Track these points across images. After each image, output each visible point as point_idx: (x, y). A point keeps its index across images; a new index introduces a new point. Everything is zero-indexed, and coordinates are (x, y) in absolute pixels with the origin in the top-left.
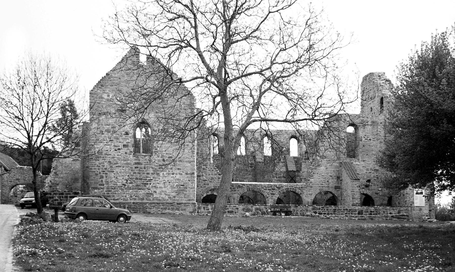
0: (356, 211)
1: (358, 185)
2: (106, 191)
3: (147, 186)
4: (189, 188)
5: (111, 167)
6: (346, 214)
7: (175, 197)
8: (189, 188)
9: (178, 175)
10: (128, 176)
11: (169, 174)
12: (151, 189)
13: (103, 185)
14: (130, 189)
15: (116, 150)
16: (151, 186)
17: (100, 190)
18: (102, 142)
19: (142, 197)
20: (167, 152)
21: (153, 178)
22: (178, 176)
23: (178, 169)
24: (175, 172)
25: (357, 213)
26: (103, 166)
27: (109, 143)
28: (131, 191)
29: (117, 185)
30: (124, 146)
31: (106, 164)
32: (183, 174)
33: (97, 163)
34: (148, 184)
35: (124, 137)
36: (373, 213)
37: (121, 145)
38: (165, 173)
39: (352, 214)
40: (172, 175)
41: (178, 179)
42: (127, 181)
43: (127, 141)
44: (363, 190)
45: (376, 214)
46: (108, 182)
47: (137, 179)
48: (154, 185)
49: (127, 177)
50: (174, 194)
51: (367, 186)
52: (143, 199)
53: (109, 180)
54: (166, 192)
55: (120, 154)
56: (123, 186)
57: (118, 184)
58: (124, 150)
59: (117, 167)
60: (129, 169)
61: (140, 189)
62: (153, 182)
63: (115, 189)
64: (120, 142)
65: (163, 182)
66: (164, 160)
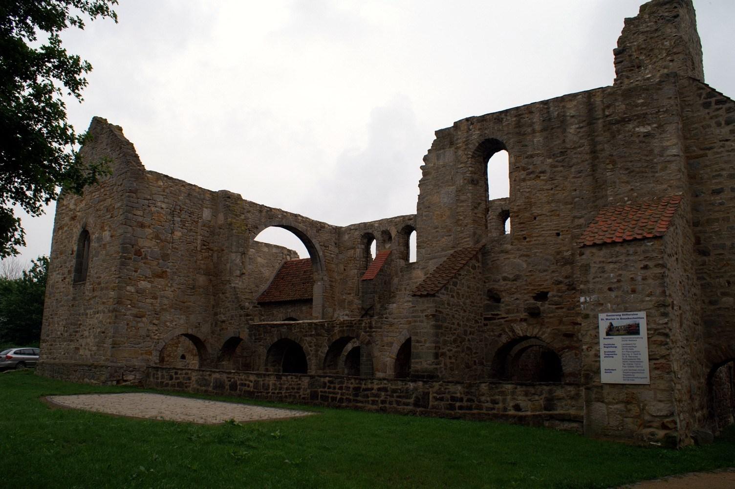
0: (407, 394)
1: (429, 312)
6: (383, 402)
25: (412, 401)
36: (458, 404)
39: (398, 403)
44: (525, 324)
45: (470, 408)
51: (534, 313)
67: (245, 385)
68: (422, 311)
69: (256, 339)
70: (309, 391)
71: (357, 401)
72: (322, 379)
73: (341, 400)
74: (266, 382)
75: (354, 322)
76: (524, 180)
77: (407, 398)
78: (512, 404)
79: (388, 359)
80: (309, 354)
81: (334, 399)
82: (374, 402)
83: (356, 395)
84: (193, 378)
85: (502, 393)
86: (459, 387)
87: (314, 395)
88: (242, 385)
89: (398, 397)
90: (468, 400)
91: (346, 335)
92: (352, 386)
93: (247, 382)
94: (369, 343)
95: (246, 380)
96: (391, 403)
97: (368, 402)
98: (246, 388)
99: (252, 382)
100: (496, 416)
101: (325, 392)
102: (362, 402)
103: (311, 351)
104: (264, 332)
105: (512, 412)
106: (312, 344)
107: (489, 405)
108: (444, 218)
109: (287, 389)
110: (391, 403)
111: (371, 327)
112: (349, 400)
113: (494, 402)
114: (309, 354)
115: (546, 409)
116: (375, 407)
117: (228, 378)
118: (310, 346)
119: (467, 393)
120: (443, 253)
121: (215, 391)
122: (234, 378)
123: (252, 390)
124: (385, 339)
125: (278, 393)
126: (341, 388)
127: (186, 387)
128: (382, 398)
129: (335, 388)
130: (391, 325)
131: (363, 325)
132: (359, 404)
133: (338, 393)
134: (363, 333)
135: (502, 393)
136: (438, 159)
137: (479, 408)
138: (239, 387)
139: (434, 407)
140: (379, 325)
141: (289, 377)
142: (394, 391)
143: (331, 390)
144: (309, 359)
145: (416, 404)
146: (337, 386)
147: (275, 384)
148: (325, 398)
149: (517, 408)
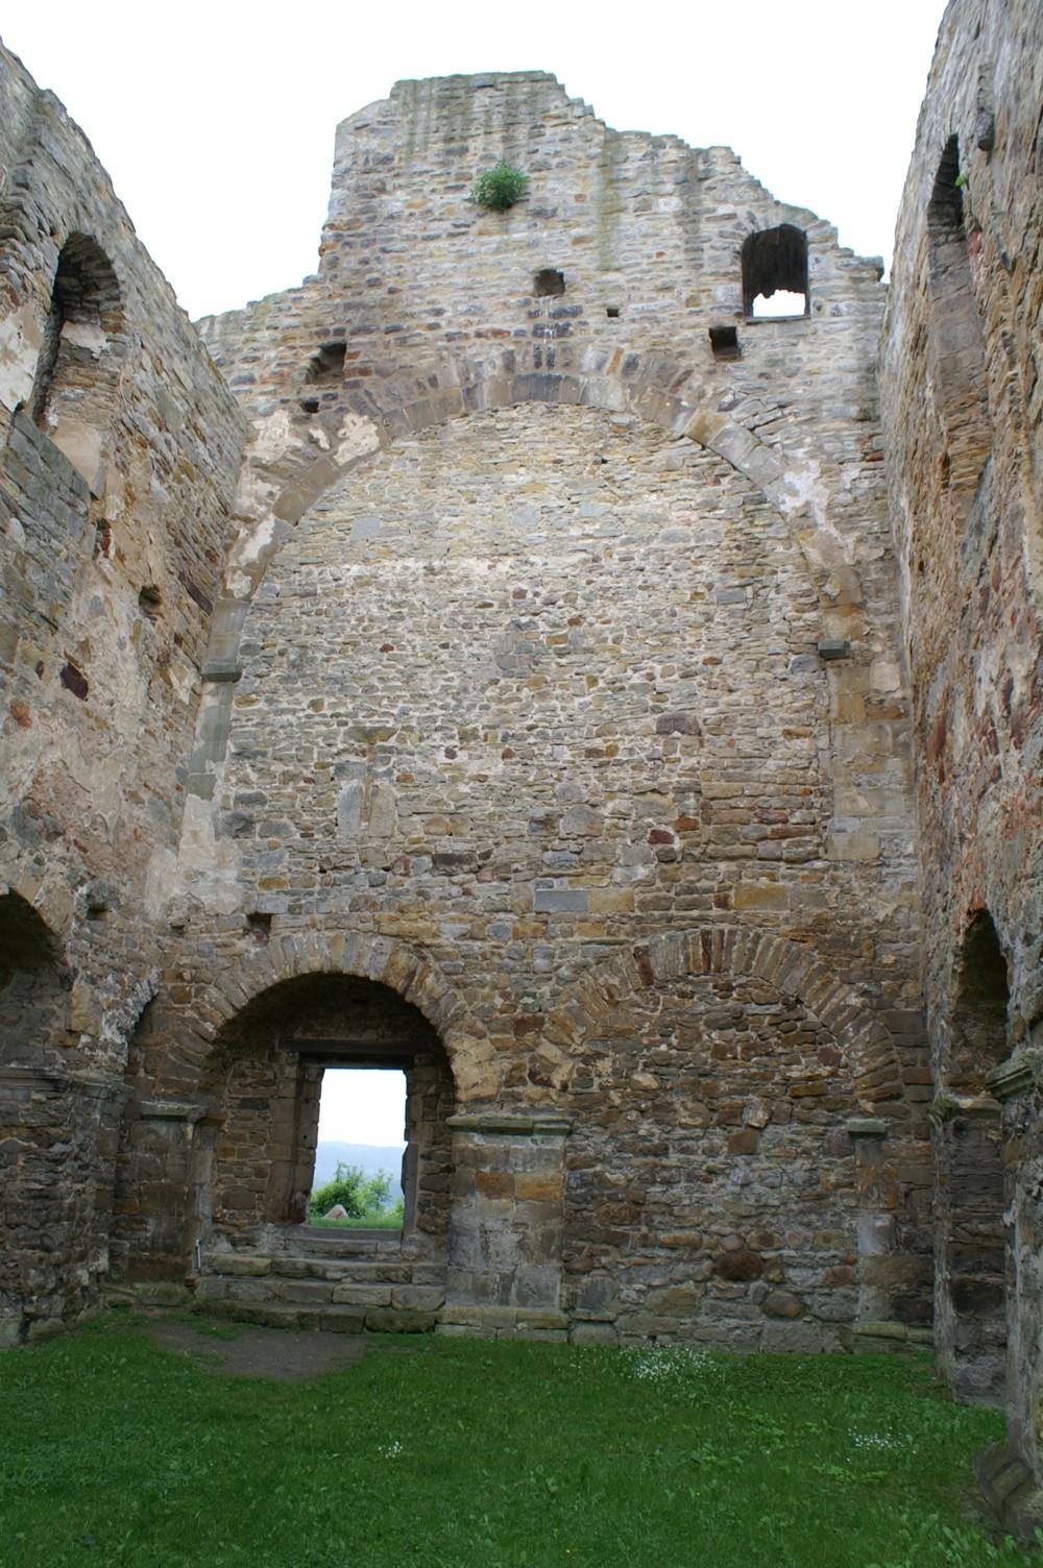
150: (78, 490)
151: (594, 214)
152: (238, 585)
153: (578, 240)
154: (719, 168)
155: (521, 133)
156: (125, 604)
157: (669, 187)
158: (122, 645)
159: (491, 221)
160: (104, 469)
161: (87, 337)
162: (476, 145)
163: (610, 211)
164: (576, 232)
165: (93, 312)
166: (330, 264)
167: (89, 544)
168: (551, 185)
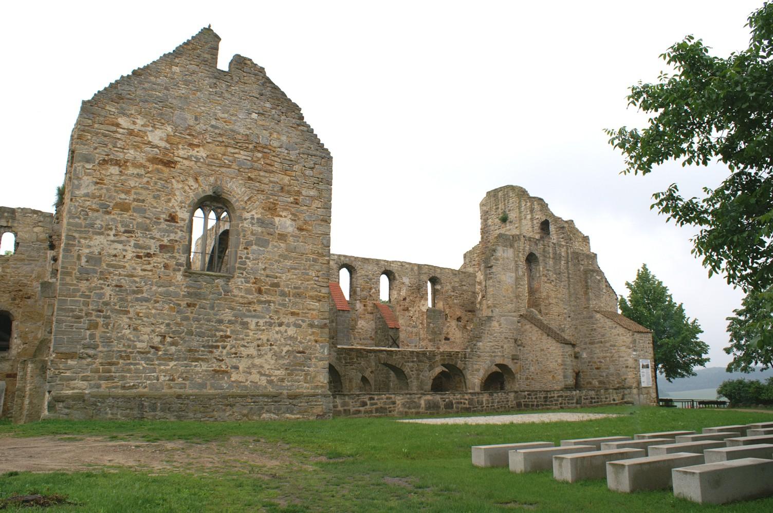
1: (569, 353)
2: (102, 364)
3: (217, 353)
4: (316, 358)
5: (122, 300)
6: (561, 404)
7: (282, 380)
8: (316, 358)
9: (292, 327)
10: (168, 325)
11: (271, 325)
12: (227, 360)
13: (95, 347)
14: (172, 360)
15: (138, 257)
16: (225, 351)
17: (85, 362)
18: (102, 234)
19: (200, 381)
20: (268, 272)
21: (232, 331)
22: (291, 331)
23: (293, 314)
24: (286, 321)
25: (575, 401)
26: (101, 296)
27: (123, 238)
28: (172, 364)
29: (135, 347)
30: (162, 247)
31: (108, 291)
32: (304, 325)
33: (84, 285)
34: (217, 347)
35: (164, 226)
36: (593, 401)
37: (154, 247)
38: (261, 322)
39: (568, 403)
40: (277, 329)
41: (291, 338)
42: (165, 337)
43: (172, 236)
46: (109, 338)
47: (190, 333)
48: (233, 350)
49: (163, 329)
50: (281, 373)
52: (203, 385)
53: (114, 335)
54: (262, 367)
55: (149, 267)
56: (153, 351)
57: (139, 345)
58: (160, 259)
59: (137, 300)
60: (171, 309)
61: (197, 360)
62: (229, 343)
63: (128, 357)
64: (154, 238)
65: (256, 343)
66: (260, 291)
67: (461, 403)
68: (567, 352)
69: (346, 363)
70: (514, 402)
71: (546, 405)
72: (523, 393)
73: (537, 406)
74: (480, 399)
75: (452, 353)
76: (546, 282)
77: (572, 400)
78: (612, 398)
79: (476, 380)
80: (411, 377)
81: (533, 405)
82: (556, 404)
83: (545, 401)
84: (398, 402)
85: (609, 394)
86: (593, 392)
87: (519, 405)
88: (458, 403)
89: (568, 400)
90: (598, 398)
91: (446, 363)
92: (542, 396)
93: (462, 401)
94: (464, 369)
95: (461, 399)
96: (565, 404)
97: (553, 405)
98: (462, 405)
99: (466, 400)
100: (608, 404)
101: (526, 401)
102: (549, 405)
103: (413, 374)
104: (357, 357)
105: (612, 402)
106: (414, 369)
107: (604, 400)
108: (509, 292)
109: (498, 402)
110: (565, 404)
111: (465, 358)
112: (542, 405)
113: (606, 398)
114: (411, 377)
115: (622, 399)
116: (557, 407)
117: (441, 398)
118: (412, 371)
119: (597, 395)
120: (510, 314)
121: (429, 412)
122: (449, 398)
123: (468, 406)
124: (474, 366)
125: (491, 406)
126: (536, 398)
127: (390, 412)
128: (560, 402)
129: (532, 398)
130: (479, 357)
131: (460, 355)
132: (549, 407)
133: (534, 401)
134: (459, 362)
135: (609, 394)
136: (504, 252)
137: (601, 401)
138: (454, 406)
139: (584, 403)
140: (471, 356)
141: (500, 394)
142: (566, 397)
143: (530, 400)
144: (411, 381)
145: (577, 403)
146: (534, 397)
147: (487, 400)
148: (526, 406)
149: (614, 400)
150: (440, 312)
151: (518, 222)
152: (478, 306)
153: (516, 228)
154: (535, 207)
155: (506, 201)
156: (454, 323)
157: (529, 212)
158: (455, 329)
159: (503, 225)
160: (444, 307)
161: (438, 287)
162: (500, 206)
163: (521, 220)
164: (516, 225)
165: (437, 282)
166: (482, 238)
167: (444, 319)
168: (512, 214)
